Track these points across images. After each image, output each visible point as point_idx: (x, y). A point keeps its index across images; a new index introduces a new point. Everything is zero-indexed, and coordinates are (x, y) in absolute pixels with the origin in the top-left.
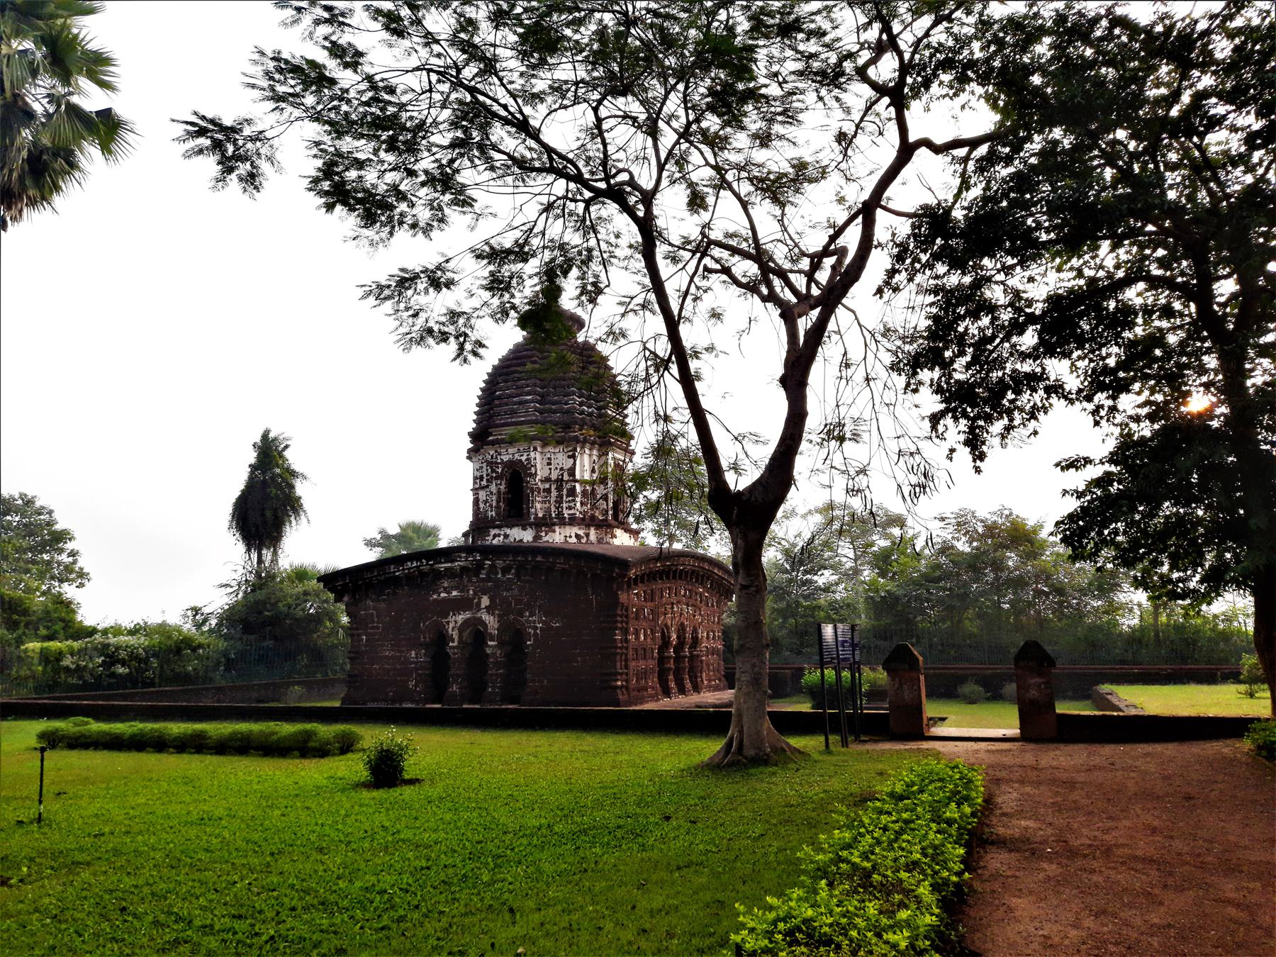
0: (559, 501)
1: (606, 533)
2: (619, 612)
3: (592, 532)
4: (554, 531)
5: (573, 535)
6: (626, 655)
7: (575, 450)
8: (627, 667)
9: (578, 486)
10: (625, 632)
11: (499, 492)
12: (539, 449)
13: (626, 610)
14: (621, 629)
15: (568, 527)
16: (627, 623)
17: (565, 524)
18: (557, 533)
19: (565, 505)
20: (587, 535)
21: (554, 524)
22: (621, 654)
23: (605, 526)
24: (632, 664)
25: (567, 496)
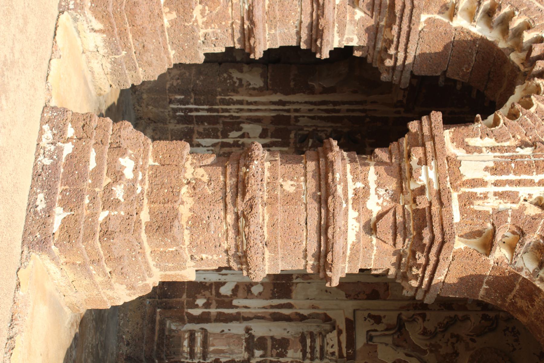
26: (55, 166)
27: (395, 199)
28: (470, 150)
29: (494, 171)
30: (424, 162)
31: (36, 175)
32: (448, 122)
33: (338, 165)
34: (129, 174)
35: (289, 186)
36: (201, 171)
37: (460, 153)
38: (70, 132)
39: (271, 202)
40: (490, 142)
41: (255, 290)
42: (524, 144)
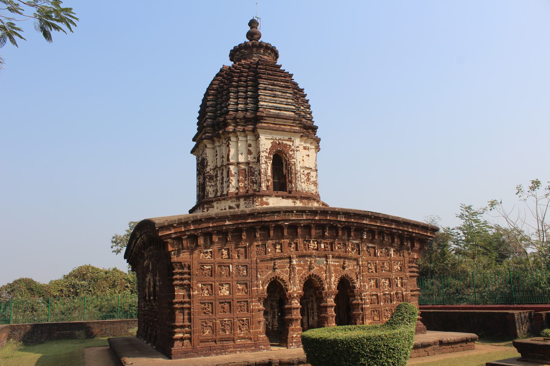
0: (222, 183)
1: (253, 201)
2: (176, 270)
3: (242, 202)
4: (213, 207)
5: (227, 208)
6: (189, 309)
7: (229, 139)
8: (190, 320)
9: (232, 168)
10: (188, 288)
11: (200, 184)
12: (208, 146)
13: (189, 268)
14: (181, 286)
15: (223, 202)
16: (189, 279)
17: (219, 200)
18: (215, 208)
19: (225, 185)
20: (238, 206)
21: (212, 202)
22: (183, 309)
23: (250, 196)
24: (198, 319)
25: (227, 178)
26: (296, 345)
27: (296, 299)
28: (291, 289)
29: (295, 286)
30: (293, 295)
31: (298, 347)
32: (287, 291)
33: (294, 307)
34: (296, 335)
35: (295, 313)
36: (293, 325)
37: (292, 290)
38: (291, 344)
39: (298, 315)
40: (290, 286)
41: (267, 317)
42: (290, 282)
